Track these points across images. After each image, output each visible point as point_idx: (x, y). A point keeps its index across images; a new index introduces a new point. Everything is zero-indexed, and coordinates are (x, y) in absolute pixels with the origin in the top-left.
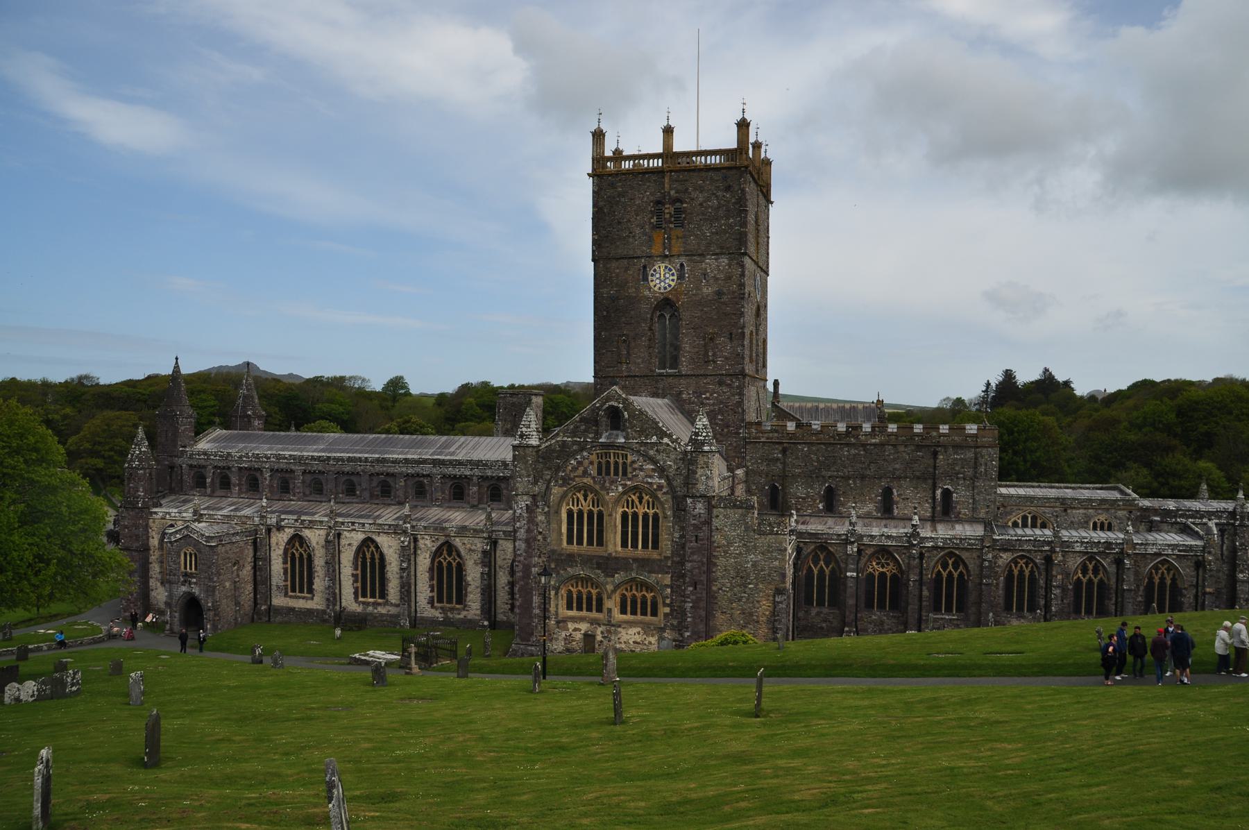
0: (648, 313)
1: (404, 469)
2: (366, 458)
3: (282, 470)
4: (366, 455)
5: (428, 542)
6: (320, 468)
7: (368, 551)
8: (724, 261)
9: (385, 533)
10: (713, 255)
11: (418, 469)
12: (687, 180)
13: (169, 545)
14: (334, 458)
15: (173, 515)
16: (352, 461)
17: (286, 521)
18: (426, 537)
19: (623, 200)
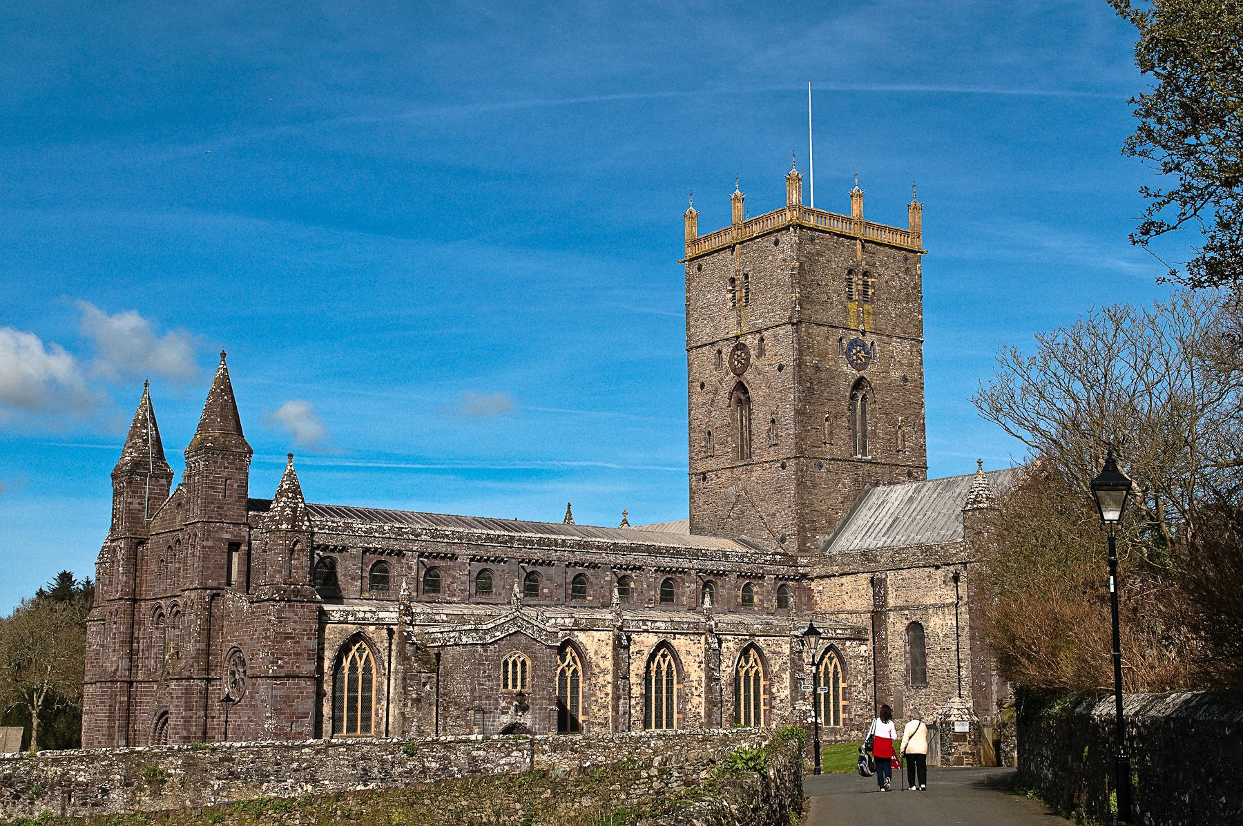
0: (847, 391)
1: (612, 558)
2: (564, 541)
3: (438, 554)
4: (563, 537)
5: (731, 645)
6: (500, 552)
7: (664, 662)
8: (907, 346)
9: (682, 634)
10: (899, 338)
11: (630, 559)
12: (874, 253)
13: (479, 648)
14: (518, 540)
15: (361, 615)
16: (544, 544)
17: (553, 621)
18: (729, 637)
19: (821, 259)
